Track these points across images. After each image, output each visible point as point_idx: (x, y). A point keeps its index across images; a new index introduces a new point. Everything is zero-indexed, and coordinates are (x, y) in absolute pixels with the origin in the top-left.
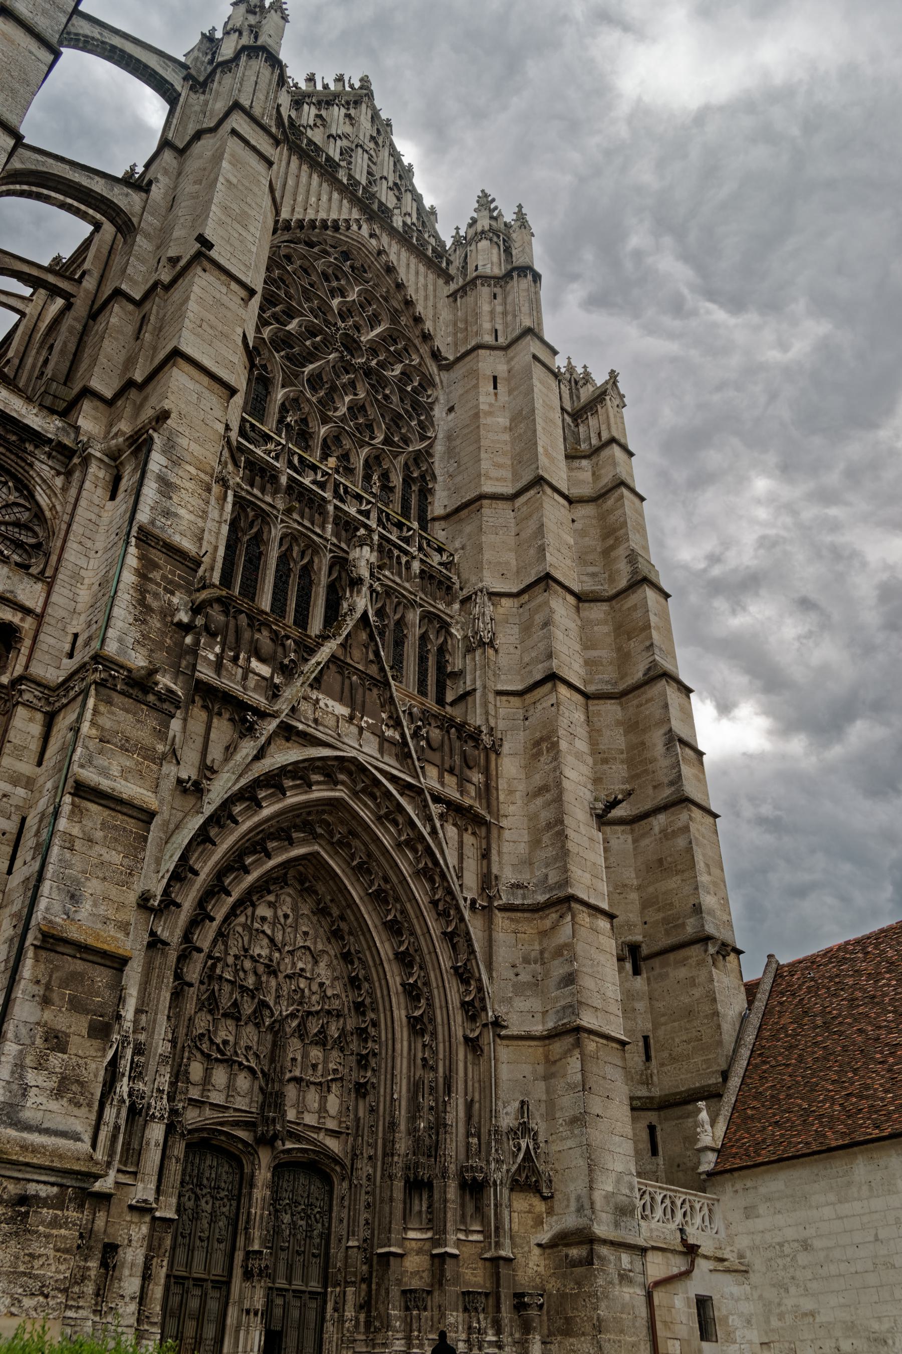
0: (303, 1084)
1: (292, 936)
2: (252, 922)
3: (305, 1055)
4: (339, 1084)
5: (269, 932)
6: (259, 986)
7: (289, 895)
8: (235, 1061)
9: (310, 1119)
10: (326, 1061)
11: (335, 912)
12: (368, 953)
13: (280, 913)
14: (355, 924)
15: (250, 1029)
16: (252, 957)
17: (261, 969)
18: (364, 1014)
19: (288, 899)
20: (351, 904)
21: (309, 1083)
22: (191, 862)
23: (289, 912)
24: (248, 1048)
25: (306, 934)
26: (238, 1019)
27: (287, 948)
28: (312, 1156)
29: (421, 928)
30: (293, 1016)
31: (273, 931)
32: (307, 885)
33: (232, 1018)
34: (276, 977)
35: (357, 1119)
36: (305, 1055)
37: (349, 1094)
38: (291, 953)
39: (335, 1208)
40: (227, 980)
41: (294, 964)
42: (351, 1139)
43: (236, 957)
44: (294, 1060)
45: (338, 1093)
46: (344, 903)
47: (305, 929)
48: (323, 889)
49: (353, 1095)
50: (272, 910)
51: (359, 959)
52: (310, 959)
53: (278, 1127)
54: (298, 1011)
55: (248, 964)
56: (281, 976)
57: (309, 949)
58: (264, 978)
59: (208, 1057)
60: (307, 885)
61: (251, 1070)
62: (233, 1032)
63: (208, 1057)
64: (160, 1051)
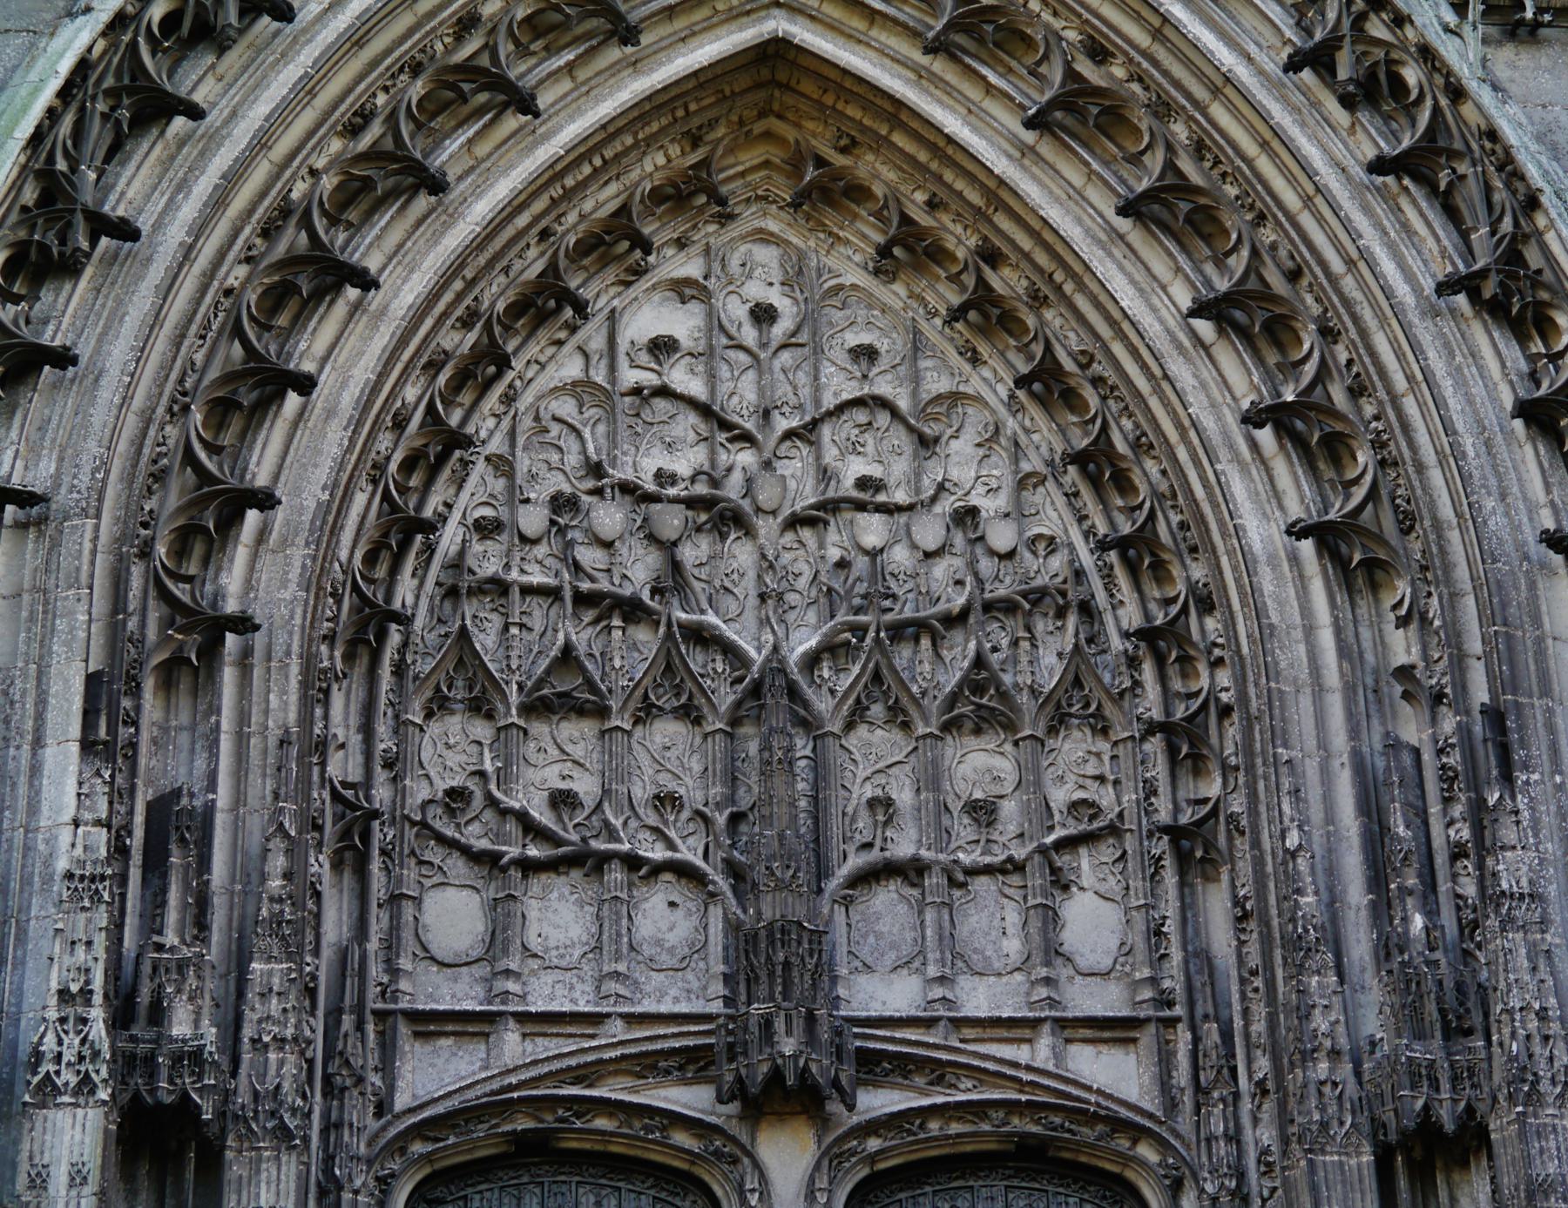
0: (933, 880)
1: (802, 378)
2: (612, 368)
3: (931, 779)
4: (1107, 852)
5: (696, 387)
6: (673, 580)
7: (764, 237)
8: (606, 858)
9: (977, 998)
10: (1030, 781)
11: (961, 241)
12: (1118, 349)
13: (736, 311)
14: (1042, 258)
15: (667, 731)
16: (627, 488)
17: (671, 521)
18: (1160, 571)
19: (766, 255)
20: (998, 193)
21: (959, 878)
22: (87, 197)
23: (776, 298)
24: (665, 801)
25: (866, 354)
26: (602, 712)
27: (782, 424)
28: (1018, 1124)
29: (1291, 180)
30: (830, 650)
31: (712, 378)
32: (810, 174)
33: (581, 711)
34: (749, 532)
35: (1199, 957)
36: (931, 779)
37: (1155, 878)
38: (806, 433)
40: (528, 590)
41: (825, 475)
42: (1183, 1038)
43: (561, 503)
44: (882, 805)
45: (1113, 885)
46: (974, 197)
47: (853, 339)
48: (891, 175)
49: (1170, 879)
50: (695, 307)
51: (1097, 381)
52: (899, 438)
53: (788, 1046)
54: (860, 630)
55: (610, 517)
56: (766, 528)
57: (883, 403)
58: (690, 554)
59: (488, 861)
60: (810, 174)
61: (684, 871)
62: (593, 763)
63: (488, 861)
64: (62, 865)
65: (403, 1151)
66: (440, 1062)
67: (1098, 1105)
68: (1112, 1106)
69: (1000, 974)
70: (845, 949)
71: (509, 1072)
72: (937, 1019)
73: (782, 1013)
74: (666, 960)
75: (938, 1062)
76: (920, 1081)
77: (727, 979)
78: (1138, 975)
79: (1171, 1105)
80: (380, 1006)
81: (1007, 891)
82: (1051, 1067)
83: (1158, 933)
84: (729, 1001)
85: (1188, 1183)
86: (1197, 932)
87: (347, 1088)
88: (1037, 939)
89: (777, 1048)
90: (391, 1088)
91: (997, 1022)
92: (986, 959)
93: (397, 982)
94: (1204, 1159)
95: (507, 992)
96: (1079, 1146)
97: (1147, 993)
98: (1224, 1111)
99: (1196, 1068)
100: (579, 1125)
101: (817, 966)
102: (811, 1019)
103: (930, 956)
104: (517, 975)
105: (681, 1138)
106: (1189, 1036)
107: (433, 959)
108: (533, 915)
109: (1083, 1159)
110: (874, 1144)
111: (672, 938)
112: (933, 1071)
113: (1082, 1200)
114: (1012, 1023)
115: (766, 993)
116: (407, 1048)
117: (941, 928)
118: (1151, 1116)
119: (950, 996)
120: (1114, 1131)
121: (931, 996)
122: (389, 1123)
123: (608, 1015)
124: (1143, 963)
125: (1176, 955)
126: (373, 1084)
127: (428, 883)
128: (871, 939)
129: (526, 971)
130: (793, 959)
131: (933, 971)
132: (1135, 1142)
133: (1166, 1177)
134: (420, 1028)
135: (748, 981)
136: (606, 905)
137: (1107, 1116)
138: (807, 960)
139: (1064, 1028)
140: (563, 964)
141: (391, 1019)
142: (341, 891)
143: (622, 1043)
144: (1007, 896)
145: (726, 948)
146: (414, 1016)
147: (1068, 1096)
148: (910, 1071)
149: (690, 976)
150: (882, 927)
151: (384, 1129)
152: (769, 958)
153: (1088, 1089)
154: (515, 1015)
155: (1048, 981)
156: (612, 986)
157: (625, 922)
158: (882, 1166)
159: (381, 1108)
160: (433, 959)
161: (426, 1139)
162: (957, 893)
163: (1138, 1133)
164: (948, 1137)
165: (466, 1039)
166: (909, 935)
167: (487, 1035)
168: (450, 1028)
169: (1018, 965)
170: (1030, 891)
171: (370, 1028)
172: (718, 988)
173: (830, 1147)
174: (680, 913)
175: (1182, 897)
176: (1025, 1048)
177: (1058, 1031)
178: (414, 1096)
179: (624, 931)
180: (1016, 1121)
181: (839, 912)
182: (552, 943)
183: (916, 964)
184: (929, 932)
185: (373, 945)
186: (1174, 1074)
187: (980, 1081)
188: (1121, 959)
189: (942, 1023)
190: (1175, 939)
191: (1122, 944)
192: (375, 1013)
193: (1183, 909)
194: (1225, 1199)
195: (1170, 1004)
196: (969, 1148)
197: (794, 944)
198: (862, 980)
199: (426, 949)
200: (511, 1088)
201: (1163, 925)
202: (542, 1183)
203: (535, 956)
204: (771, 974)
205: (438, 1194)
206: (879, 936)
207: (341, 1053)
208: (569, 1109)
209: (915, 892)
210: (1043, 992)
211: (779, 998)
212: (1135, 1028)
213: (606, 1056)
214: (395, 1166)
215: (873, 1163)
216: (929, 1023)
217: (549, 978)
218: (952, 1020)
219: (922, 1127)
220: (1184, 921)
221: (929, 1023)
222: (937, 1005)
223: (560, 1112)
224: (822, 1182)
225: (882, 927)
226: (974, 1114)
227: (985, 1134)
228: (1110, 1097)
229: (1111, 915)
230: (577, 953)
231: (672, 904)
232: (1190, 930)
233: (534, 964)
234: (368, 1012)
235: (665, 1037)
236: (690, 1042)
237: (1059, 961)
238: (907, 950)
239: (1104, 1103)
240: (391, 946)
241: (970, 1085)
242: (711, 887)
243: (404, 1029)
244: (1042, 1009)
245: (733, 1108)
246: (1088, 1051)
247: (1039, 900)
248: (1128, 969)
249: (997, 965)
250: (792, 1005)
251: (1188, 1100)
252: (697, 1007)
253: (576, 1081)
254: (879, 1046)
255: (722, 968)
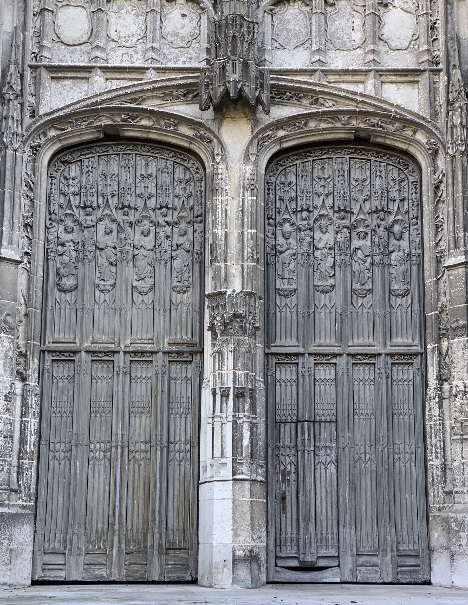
39: (427, 208)
42: (443, 77)
65: (45, 134)
66: (64, 92)
67: (396, 112)
68: (402, 113)
69: (350, 50)
70: (270, 38)
71: (97, 96)
72: (315, 71)
73: (231, 62)
74: (179, 43)
75: (315, 91)
76: (305, 102)
77: (208, 50)
78: (421, 49)
79: (435, 114)
80: (34, 63)
81: (355, 8)
82: (373, 94)
83: (433, 28)
84: (208, 61)
85: (441, 153)
86: (453, 28)
87: (11, 100)
88: (369, 30)
89: (227, 79)
90: (38, 103)
91: (346, 72)
92: (343, 42)
93: (42, 52)
94: (449, 138)
95: (97, 57)
96: (386, 135)
97: (425, 58)
98: (461, 112)
99: (448, 93)
100: (133, 123)
101: (251, 40)
102: (246, 65)
103: (314, 40)
104: (103, 50)
105: (184, 130)
106: (446, 78)
107: (62, 42)
108: (113, 20)
109: (388, 142)
110: (281, 133)
111: (183, 32)
112: (312, 97)
113: (387, 164)
114: (354, 72)
115: (224, 53)
116: (47, 84)
117: (319, 25)
118: (423, 119)
119: (323, 59)
120: (404, 127)
121: (313, 60)
122: (37, 120)
123: (148, 69)
124: (424, 42)
125: (441, 38)
126: (29, 102)
127: (60, 5)
128: (285, 33)
129: (109, 49)
130: (237, 34)
131: (314, 47)
132: (415, 132)
133: (429, 149)
134: (54, 75)
135: (216, 48)
136: (149, 14)
137: (400, 118)
138: (246, 36)
139: (381, 75)
140: (128, 45)
141: (39, 70)
142: (13, 6)
143: (154, 82)
144: (355, 11)
145: (209, 36)
146: (51, 69)
147: (381, 108)
148: (301, 98)
149: (191, 51)
150: (290, 27)
151: (34, 123)
152: (226, 35)
153: (392, 105)
154: (100, 68)
155: (373, 51)
156: (150, 54)
157: (158, 23)
158: (285, 145)
159: (33, 113)
160: (62, 42)
161: (57, 129)
162: (330, 9)
163: (416, 126)
164: (319, 130)
165: (78, 80)
166: (304, 31)
167: (88, 79)
168: (69, 75)
169: (359, 45)
170: (367, 7)
171: (28, 74)
172: (204, 55)
173: (257, 134)
174: (187, 20)
175: (446, 9)
176: (361, 86)
177: (378, 77)
178: (51, 108)
179: (158, 28)
180: (354, 122)
181: (268, 18)
182: (122, 35)
183: (307, 45)
184: (313, 28)
185: (30, 33)
186: (437, 99)
187: (336, 102)
188: (413, 42)
189: (318, 72)
190: (441, 30)
191: (414, 34)
192: (30, 67)
193: (446, 14)
194: (458, 156)
195: (437, 64)
196: (330, 137)
197: (238, 26)
198: (279, 52)
199: (59, 38)
200: (97, 103)
201: (435, 23)
202: (119, 154)
203: (113, 40)
204: (226, 44)
205: (66, 158)
206: (288, 31)
207: (8, 83)
208: (128, 115)
209: (308, 9)
210: (371, 57)
211: (230, 54)
212: (419, 75)
213: (145, 88)
214: (38, 141)
215: (281, 143)
216: (312, 72)
217: (121, 51)
218: (323, 71)
219: (306, 124)
220: (447, 21)
221: (312, 72)
222: (315, 64)
223: (123, 116)
224: (253, 150)
225: (290, 27)
226: (333, 119)
227: (338, 128)
228: (403, 109)
229: (409, 20)
230: (135, 40)
231: (184, 15)
232: (449, 26)
233: (113, 45)
234: (26, 67)
235: (176, 79)
236: (188, 81)
237: (381, 43)
238: (302, 38)
239: (398, 111)
240: (40, 35)
241: (331, 104)
242: (201, 5)
243: (45, 75)
244: (370, 66)
245: (209, 114)
246: (394, 87)
247: (371, 11)
248: (416, 47)
249: (349, 45)
250: (236, 58)
251: (443, 111)
252: (195, 65)
253: (133, 101)
254: (284, 84)
255: (206, 45)
